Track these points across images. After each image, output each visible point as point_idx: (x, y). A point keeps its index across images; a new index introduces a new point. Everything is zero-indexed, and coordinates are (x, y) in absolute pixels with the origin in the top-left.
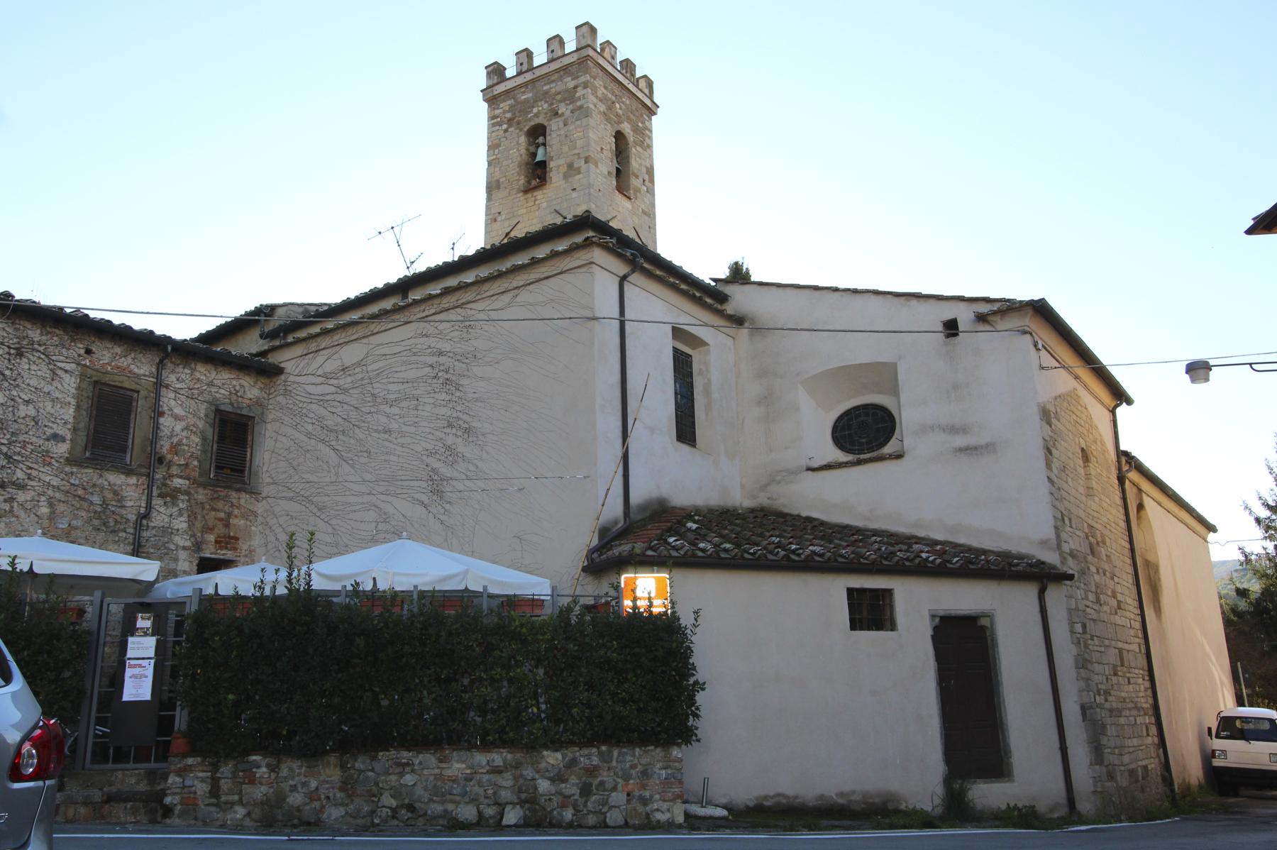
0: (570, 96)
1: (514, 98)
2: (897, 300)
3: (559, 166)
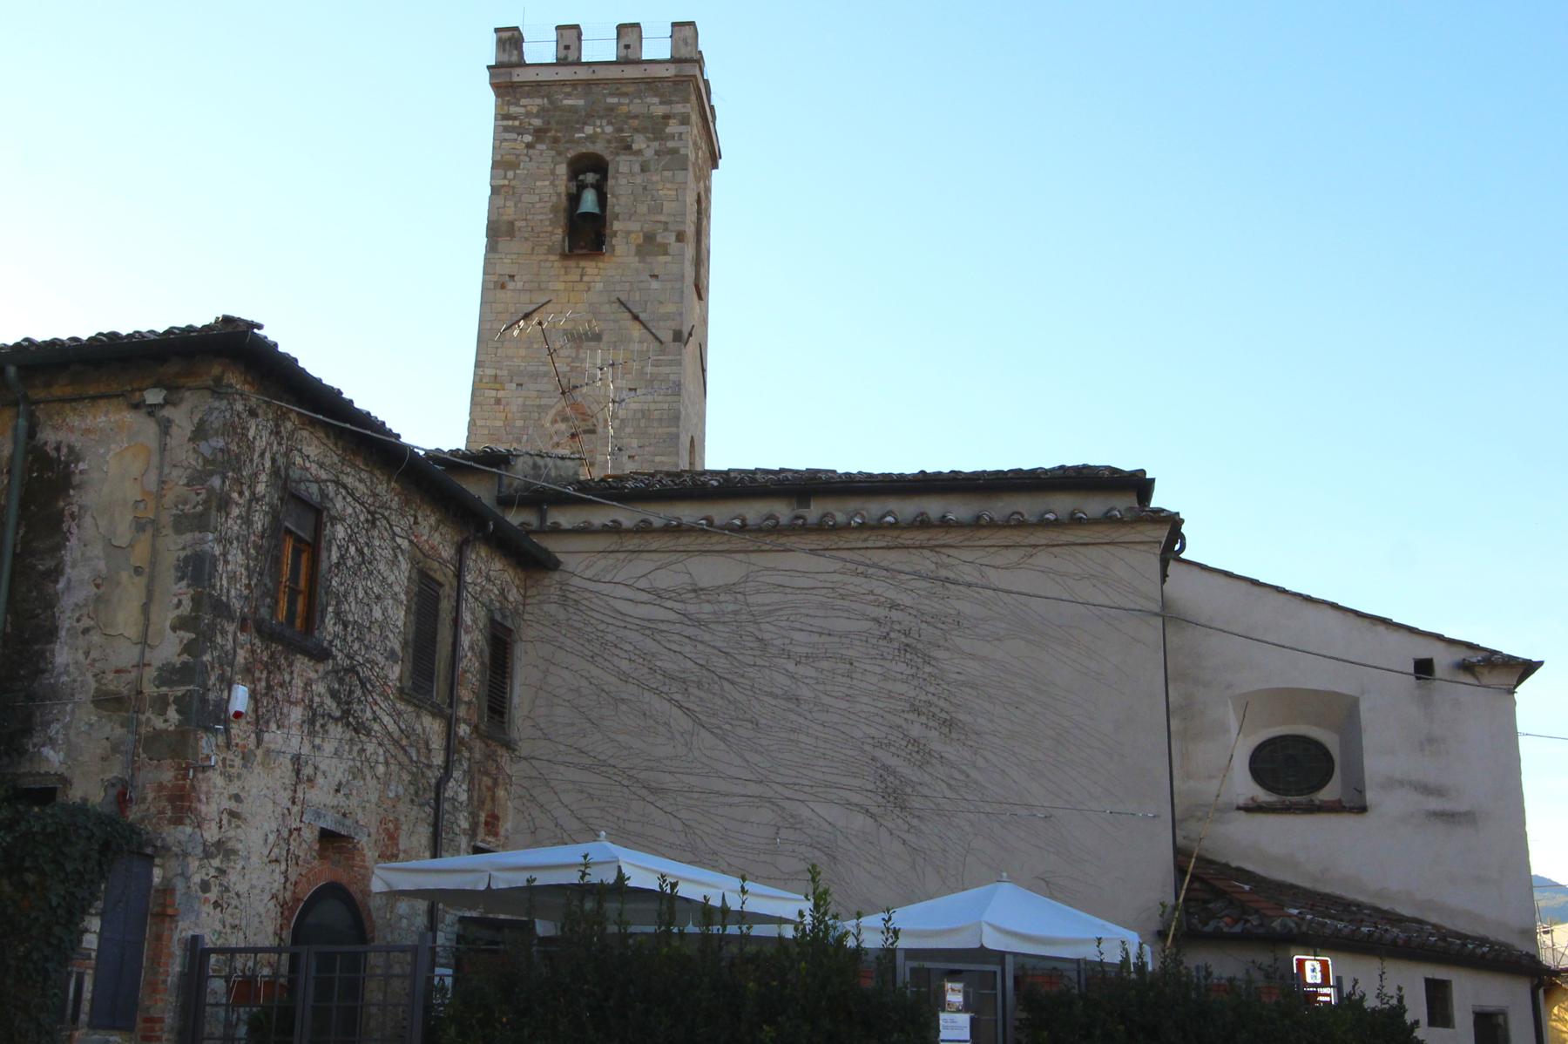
0: (656, 127)
1: (548, 98)
2: (1359, 621)
3: (628, 233)
